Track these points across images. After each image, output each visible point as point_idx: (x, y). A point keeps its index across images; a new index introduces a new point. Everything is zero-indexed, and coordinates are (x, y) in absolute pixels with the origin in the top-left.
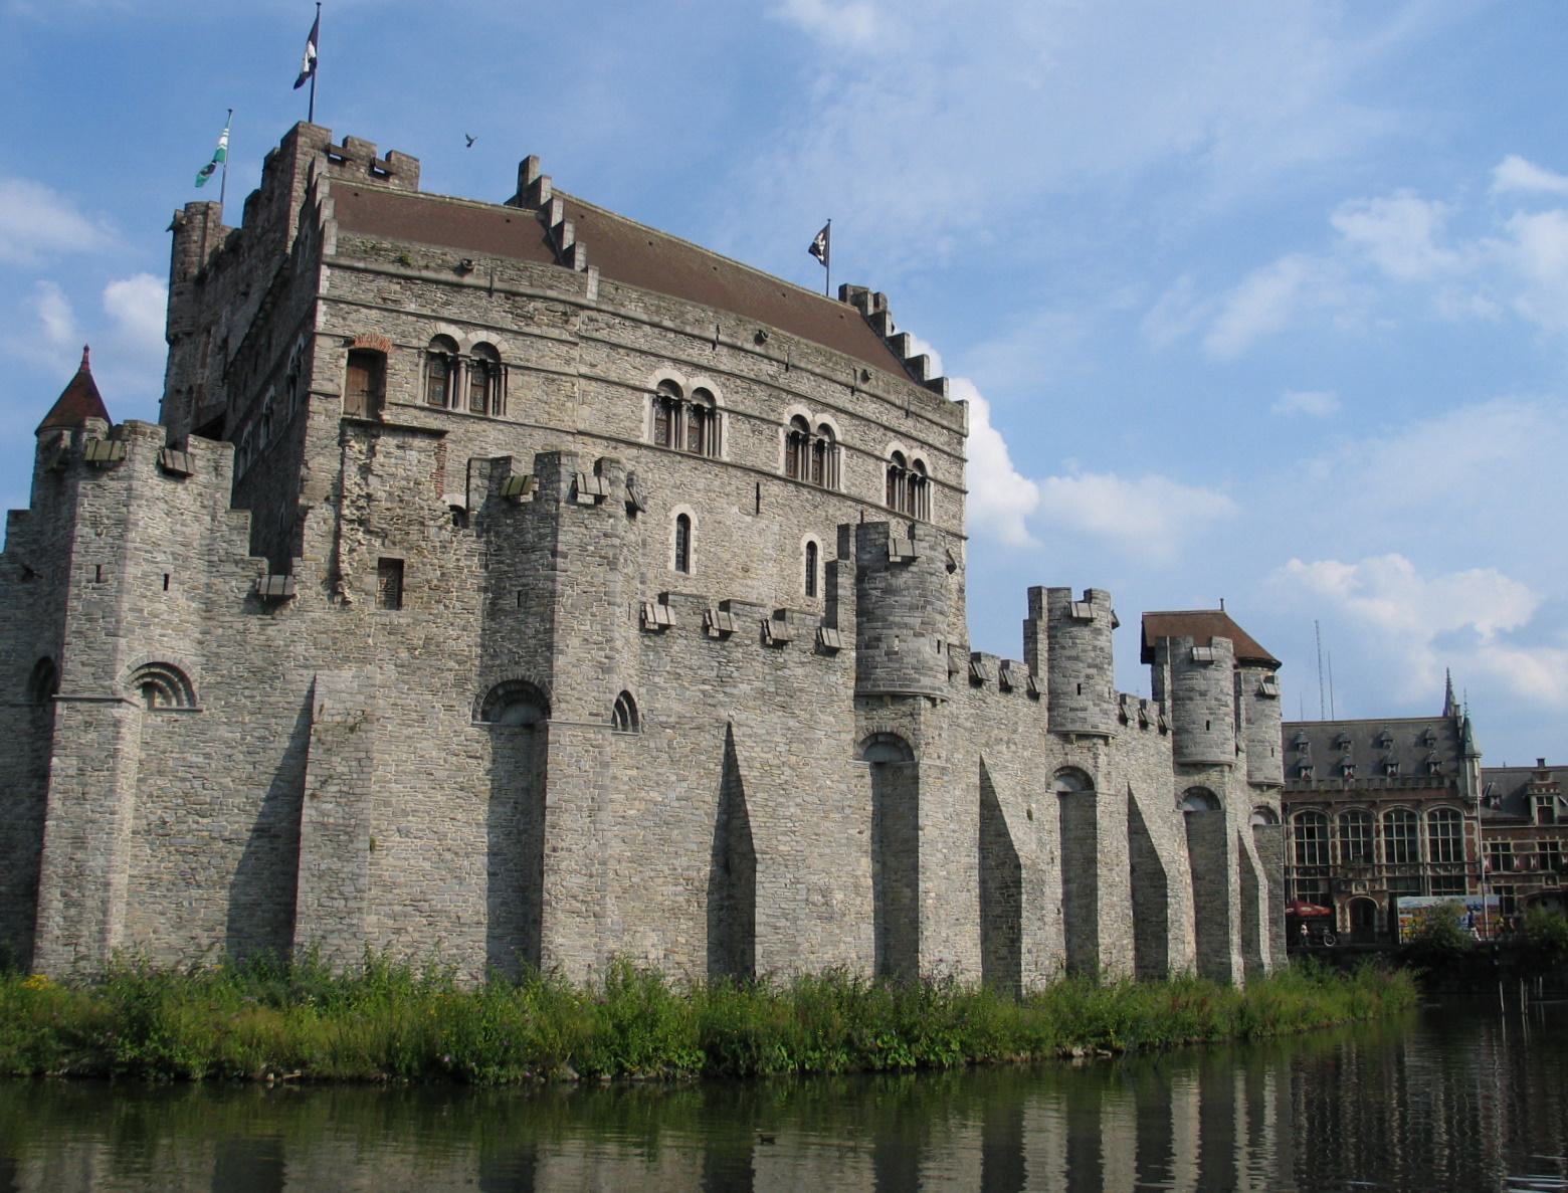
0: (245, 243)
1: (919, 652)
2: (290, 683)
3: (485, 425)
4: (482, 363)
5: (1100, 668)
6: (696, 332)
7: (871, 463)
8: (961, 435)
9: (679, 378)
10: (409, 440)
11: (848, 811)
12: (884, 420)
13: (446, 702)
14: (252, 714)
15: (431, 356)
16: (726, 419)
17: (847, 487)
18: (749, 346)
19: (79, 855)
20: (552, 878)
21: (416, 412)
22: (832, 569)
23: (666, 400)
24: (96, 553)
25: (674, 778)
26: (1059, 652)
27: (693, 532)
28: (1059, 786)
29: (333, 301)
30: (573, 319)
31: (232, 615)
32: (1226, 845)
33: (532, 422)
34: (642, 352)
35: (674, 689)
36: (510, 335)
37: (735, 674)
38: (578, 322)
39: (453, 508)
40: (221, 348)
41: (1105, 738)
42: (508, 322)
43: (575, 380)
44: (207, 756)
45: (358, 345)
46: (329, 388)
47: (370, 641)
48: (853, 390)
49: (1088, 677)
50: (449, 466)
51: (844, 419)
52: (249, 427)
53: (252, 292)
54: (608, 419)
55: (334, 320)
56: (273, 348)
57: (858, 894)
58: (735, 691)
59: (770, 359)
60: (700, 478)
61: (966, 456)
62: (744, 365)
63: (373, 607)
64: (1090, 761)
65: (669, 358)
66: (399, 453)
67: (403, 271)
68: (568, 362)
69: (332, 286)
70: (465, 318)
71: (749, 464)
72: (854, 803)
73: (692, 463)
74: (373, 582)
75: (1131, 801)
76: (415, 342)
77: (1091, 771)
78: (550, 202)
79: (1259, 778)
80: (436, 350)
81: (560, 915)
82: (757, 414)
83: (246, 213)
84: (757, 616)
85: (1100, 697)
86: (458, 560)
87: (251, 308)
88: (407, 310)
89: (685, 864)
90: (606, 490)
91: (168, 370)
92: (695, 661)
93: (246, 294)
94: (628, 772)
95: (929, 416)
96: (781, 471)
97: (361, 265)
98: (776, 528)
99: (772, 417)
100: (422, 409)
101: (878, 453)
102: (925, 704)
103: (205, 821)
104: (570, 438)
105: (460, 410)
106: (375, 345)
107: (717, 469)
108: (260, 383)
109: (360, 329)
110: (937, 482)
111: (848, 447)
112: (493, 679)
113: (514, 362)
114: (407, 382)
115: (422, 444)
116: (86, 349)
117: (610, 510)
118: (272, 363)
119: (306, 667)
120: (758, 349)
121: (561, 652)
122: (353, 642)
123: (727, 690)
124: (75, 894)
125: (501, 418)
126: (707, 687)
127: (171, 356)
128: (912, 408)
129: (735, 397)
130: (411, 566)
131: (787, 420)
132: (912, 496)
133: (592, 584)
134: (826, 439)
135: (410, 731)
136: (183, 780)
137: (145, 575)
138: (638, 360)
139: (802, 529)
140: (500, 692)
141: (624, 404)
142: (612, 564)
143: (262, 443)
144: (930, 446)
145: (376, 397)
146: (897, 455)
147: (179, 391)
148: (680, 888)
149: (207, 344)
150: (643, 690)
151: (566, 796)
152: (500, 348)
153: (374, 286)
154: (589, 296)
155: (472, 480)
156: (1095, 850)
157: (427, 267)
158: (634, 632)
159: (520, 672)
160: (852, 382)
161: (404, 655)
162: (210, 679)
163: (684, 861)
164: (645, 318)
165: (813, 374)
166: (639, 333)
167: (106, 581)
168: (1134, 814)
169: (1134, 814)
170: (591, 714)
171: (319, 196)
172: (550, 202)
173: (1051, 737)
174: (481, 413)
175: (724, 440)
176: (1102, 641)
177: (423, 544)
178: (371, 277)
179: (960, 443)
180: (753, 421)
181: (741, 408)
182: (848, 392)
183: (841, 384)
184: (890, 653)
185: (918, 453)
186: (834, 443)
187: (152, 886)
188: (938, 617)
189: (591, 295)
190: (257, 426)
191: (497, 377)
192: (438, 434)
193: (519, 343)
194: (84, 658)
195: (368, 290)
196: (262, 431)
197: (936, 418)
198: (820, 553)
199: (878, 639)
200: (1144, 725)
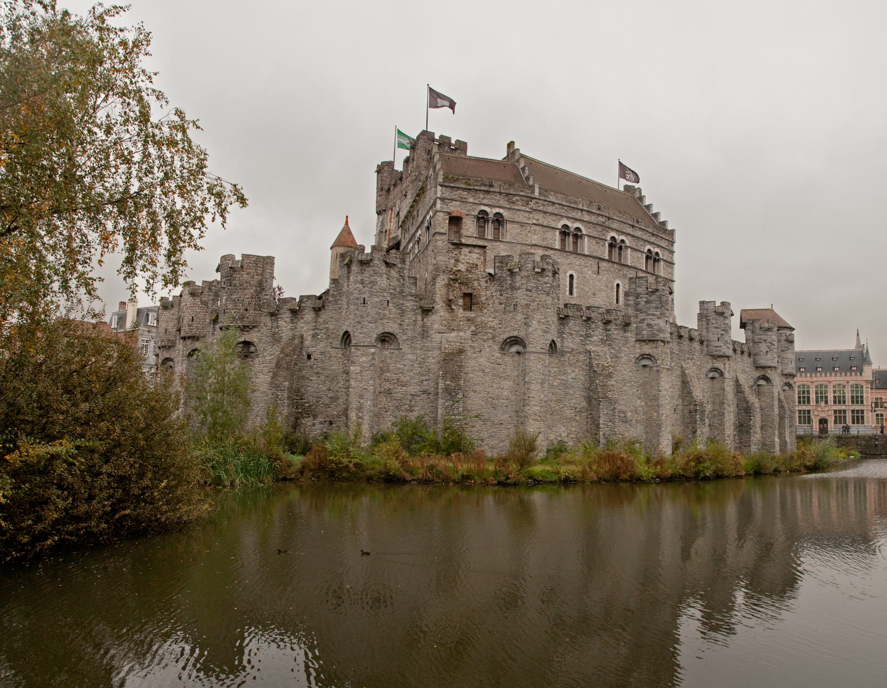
0: (404, 177)
1: (659, 324)
2: (431, 338)
3: (498, 243)
4: (497, 220)
5: (726, 331)
6: (575, 206)
7: (639, 254)
8: (672, 243)
9: (569, 224)
10: (473, 249)
11: (633, 383)
12: (644, 237)
13: (489, 344)
14: (420, 350)
15: (478, 219)
16: (586, 239)
18: (594, 211)
19: (362, 401)
20: (528, 408)
21: (474, 239)
22: (626, 294)
23: (564, 232)
24: (363, 294)
26: (711, 325)
27: (575, 281)
28: (711, 375)
29: (442, 199)
30: (530, 203)
31: (412, 315)
32: (773, 398)
33: (516, 241)
34: (556, 215)
36: (507, 210)
37: (592, 333)
38: (532, 204)
39: (490, 274)
40: (397, 216)
41: (728, 357)
42: (506, 204)
43: (531, 226)
44: (405, 365)
45: (453, 215)
46: (442, 231)
47: (461, 323)
48: (633, 226)
50: (488, 258)
51: (629, 237)
52: (411, 245)
53: (408, 194)
54: (544, 240)
55: (443, 206)
56: (419, 216)
57: (637, 413)
58: (592, 340)
59: (602, 215)
60: (577, 261)
61: (675, 250)
62: (593, 219)
63: (461, 311)
65: (565, 217)
66: (469, 255)
67: (468, 187)
68: (528, 219)
69: (442, 193)
70: (491, 203)
71: (595, 255)
72: (635, 380)
73: (574, 255)
74: (461, 302)
75: (737, 381)
76: (473, 213)
78: (519, 159)
79: (786, 372)
80: (481, 216)
81: (530, 420)
82: (597, 236)
83: (404, 165)
84: (600, 312)
85: (726, 342)
87: (409, 200)
89: (575, 402)
90: (546, 267)
91: (377, 224)
92: (577, 328)
93: (406, 195)
94: (554, 369)
95: (661, 235)
96: (607, 258)
97: (453, 185)
98: (605, 279)
99: (604, 237)
100: (476, 238)
101: (642, 250)
102: (662, 344)
103: (404, 388)
104: (530, 247)
105: (490, 237)
108: (415, 229)
109: (453, 209)
110: (664, 260)
111: (631, 248)
112: (506, 336)
114: (469, 227)
115: (478, 251)
116: (347, 217)
117: (547, 274)
118: (419, 222)
119: (439, 333)
120: (598, 212)
121: (530, 326)
122: (455, 323)
123: (589, 339)
124: (361, 415)
125: (504, 240)
127: (378, 219)
128: (655, 233)
129: (590, 230)
130: (475, 296)
131: (609, 238)
132: (654, 266)
133: (541, 301)
134: (623, 245)
135: (475, 355)
136: (395, 374)
137: (381, 301)
138: (554, 218)
139: (615, 279)
140: (508, 341)
141: (549, 234)
142: (548, 294)
143: (416, 251)
144: (661, 247)
145: (458, 233)
146: (649, 250)
147: (382, 232)
148: (572, 411)
149: (391, 214)
150: (559, 340)
152: (504, 215)
153: (457, 193)
154: (536, 194)
155: (496, 264)
156: (724, 399)
157: (476, 186)
158: (555, 319)
159: (515, 334)
160: (632, 223)
161: (473, 328)
162: (404, 337)
163: (574, 401)
164: (556, 201)
165: (618, 221)
166: (554, 208)
167: (367, 303)
168: (737, 384)
169: (737, 384)
171: (435, 160)
172: (519, 159)
173: (708, 357)
174: (496, 239)
175: (586, 246)
176: (727, 321)
177: (479, 287)
178: (455, 189)
179: (672, 245)
181: (592, 234)
182: (631, 227)
183: (628, 224)
184: (649, 325)
185: (657, 250)
186: (627, 247)
187: (386, 412)
188: (666, 312)
189: (537, 193)
190: (414, 245)
191: (503, 226)
192: (484, 247)
193: (510, 212)
194: (360, 331)
195: (456, 194)
196: (416, 246)
197: (663, 236)
198: (621, 288)
199: (644, 320)
200: (742, 353)
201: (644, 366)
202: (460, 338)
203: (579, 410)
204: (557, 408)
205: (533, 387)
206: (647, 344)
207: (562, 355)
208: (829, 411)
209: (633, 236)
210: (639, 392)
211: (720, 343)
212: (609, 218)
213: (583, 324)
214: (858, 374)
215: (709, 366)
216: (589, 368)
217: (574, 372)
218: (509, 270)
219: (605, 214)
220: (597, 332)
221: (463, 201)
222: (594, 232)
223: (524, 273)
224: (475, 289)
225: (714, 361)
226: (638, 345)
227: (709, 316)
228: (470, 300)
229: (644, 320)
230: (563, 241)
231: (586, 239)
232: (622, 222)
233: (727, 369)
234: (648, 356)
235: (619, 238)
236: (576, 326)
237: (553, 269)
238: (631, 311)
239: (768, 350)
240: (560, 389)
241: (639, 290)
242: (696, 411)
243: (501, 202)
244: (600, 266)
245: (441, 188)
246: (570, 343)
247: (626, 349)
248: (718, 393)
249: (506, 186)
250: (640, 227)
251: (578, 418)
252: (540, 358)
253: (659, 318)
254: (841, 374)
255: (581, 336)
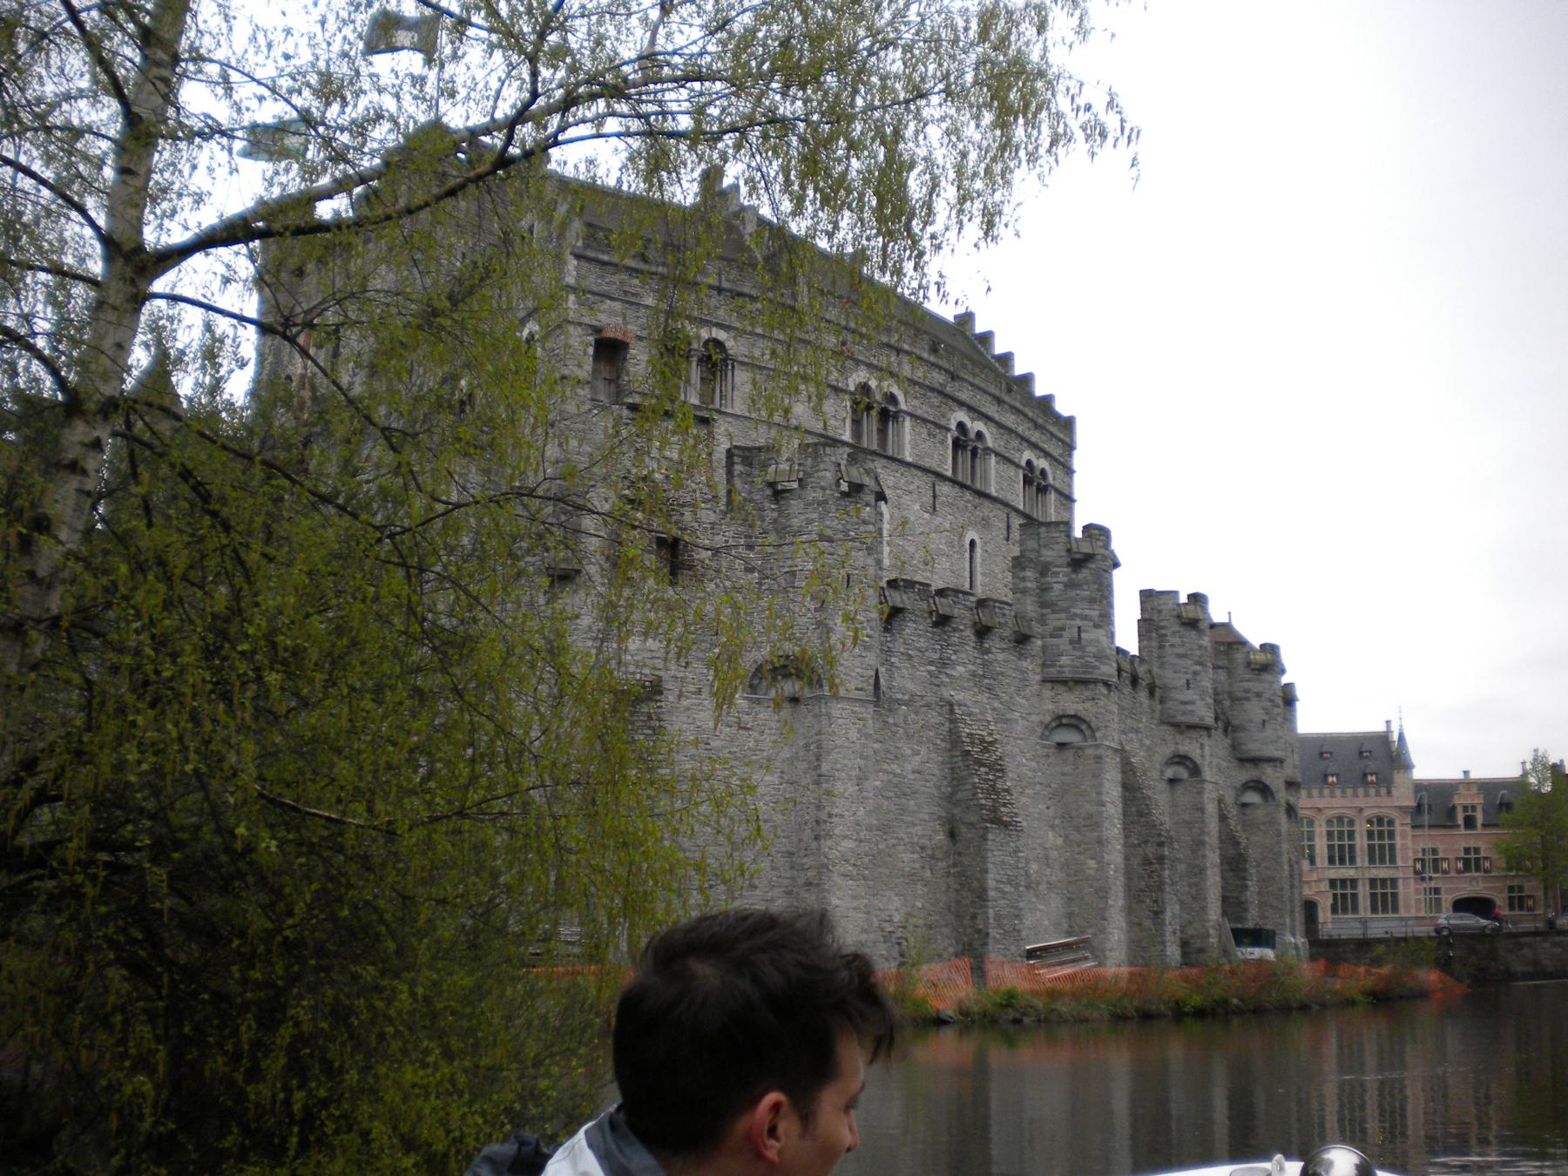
1: (1098, 642)
8: (1070, 447)
11: (1038, 787)
16: (908, 423)
17: (997, 491)
18: (925, 355)
20: (829, 843)
25: (909, 752)
26: (1169, 650)
28: (1170, 773)
35: (907, 669)
37: (953, 657)
48: (999, 401)
49: (1195, 673)
57: (1048, 866)
59: (940, 368)
64: (1198, 751)
67: (642, 266)
69: (579, 277)
71: (927, 465)
77: (1198, 760)
81: (835, 877)
82: (931, 418)
86: (727, 541)
88: (646, 303)
92: (922, 644)
97: (605, 258)
99: (943, 422)
102: (1104, 690)
106: (620, 336)
107: (902, 469)
111: (997, 454)
113: (740, 359)
120: (932, 359)
123: (949, 672)
125: (729, 410)
126: (933, 668)
128: (1040, 421)
129: (915, 402)
131: (953, 426)
134: (980, 445)
146: (1029, 463)
148: (916, 856)
151: (839, 766)
153: (616, 278)
160: (997, 393)
163: (918, 830)
165: (972, 384)
170: (857, 689)
173: (1165, 727)
177: (696, 525)
178: (612, 269)
179: (1070, 455)
180: (929, 425)
181: (919, 412)
183: (990, 394)
186: (987, 450)
191: (724, 378)
199: (1063, 629)
201: (1061, 746)
202: (649, 655)
203: (929, 852)
204: (882, 846)
205: (839, 787)
206: (1070, 690)
207: (890, 710)
208: (1319, 881)
209: (999, 425)
210: (1051, 811)
211: (1190, 695)
212: (954, 377)
213: (933, 633)
214: (1383, 791)
215: (1168, 751)
216: (948, 746)
217: (917, 753)
218: (772, 485)
219: (946, 365)
220: (964, 656)
221: (630, 300)
222: (924, 407)
223: (812, 494)
224: (686, 529)
225: (1179, 737)
226: (1047, 693)
227: (1163, 627)
228: (673, 553)
229: (1063, 629)
230: (857, 423)
231: (908, 423)
232: (980, 388)
233: (1208, 758)
234: (1073, 721)
235: (976, 426)
236: (920, 636)
237: (878, 489)
238: (1030, 607)
239: (1266, 717)
240: (888, 798)
241: (1048, 555)
242: (1161, 859)
243: (721, 312)
244: (938, 493)
245: (575, 262)
246: (906, 680)
247: (1023, 701)
248: (1187, 817)
249: (734, 274)
250: (1013, 403)
251: (928, 874)
252: (853, 712)
253: (1097, 626)
254: (1343, 792)
255: (931, 663)
